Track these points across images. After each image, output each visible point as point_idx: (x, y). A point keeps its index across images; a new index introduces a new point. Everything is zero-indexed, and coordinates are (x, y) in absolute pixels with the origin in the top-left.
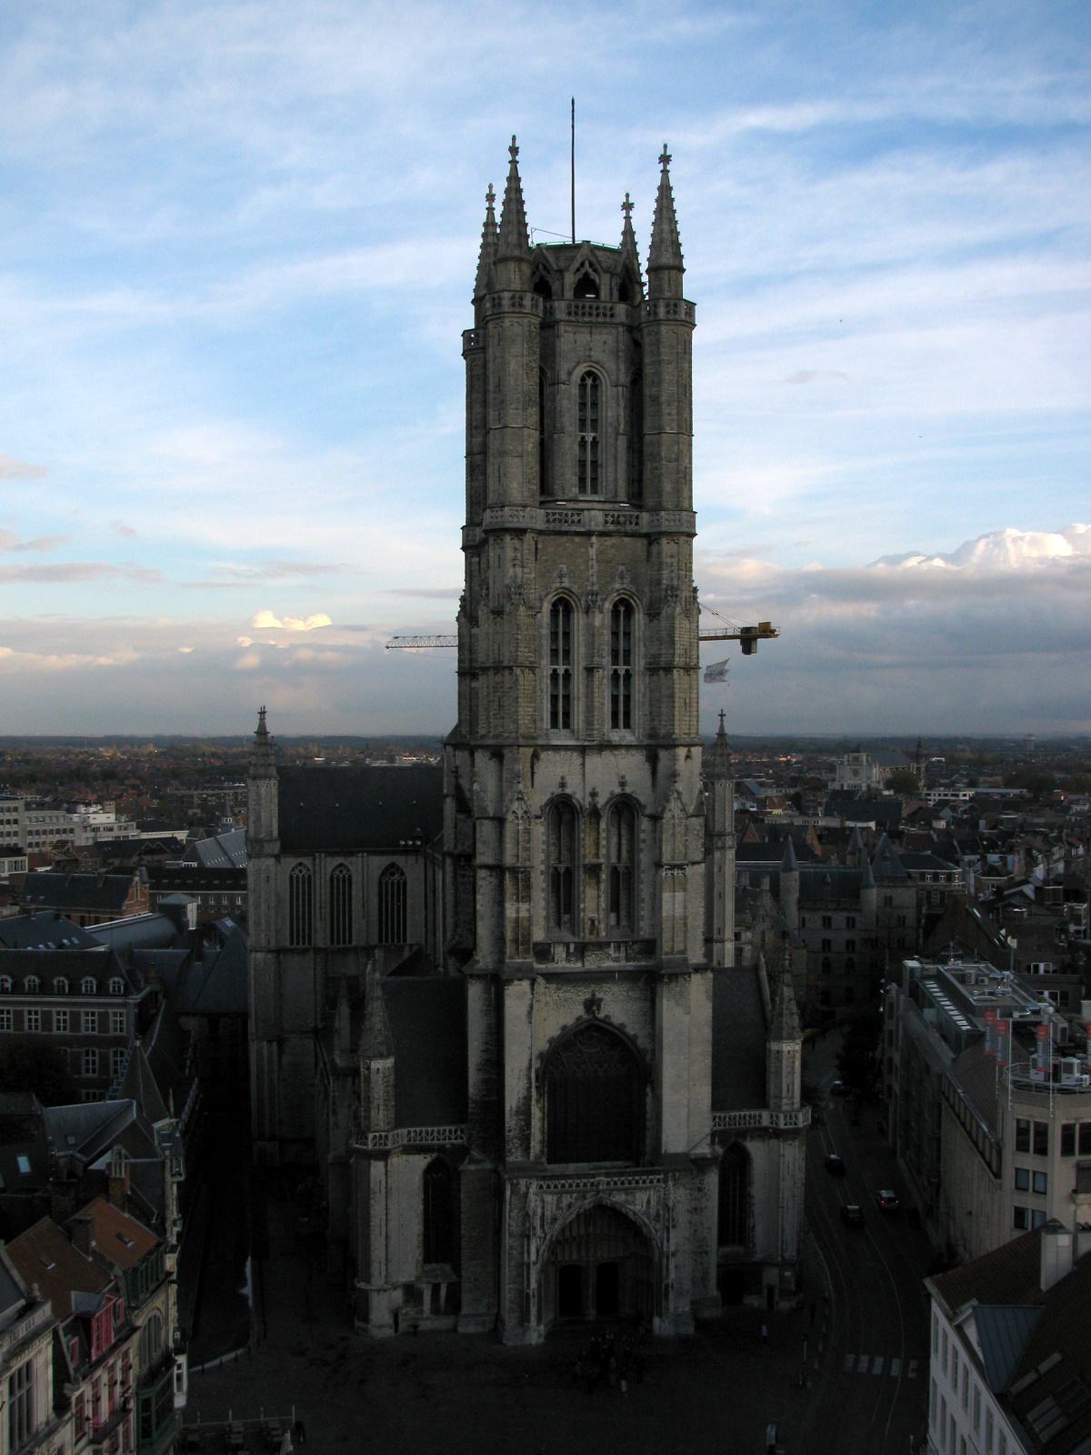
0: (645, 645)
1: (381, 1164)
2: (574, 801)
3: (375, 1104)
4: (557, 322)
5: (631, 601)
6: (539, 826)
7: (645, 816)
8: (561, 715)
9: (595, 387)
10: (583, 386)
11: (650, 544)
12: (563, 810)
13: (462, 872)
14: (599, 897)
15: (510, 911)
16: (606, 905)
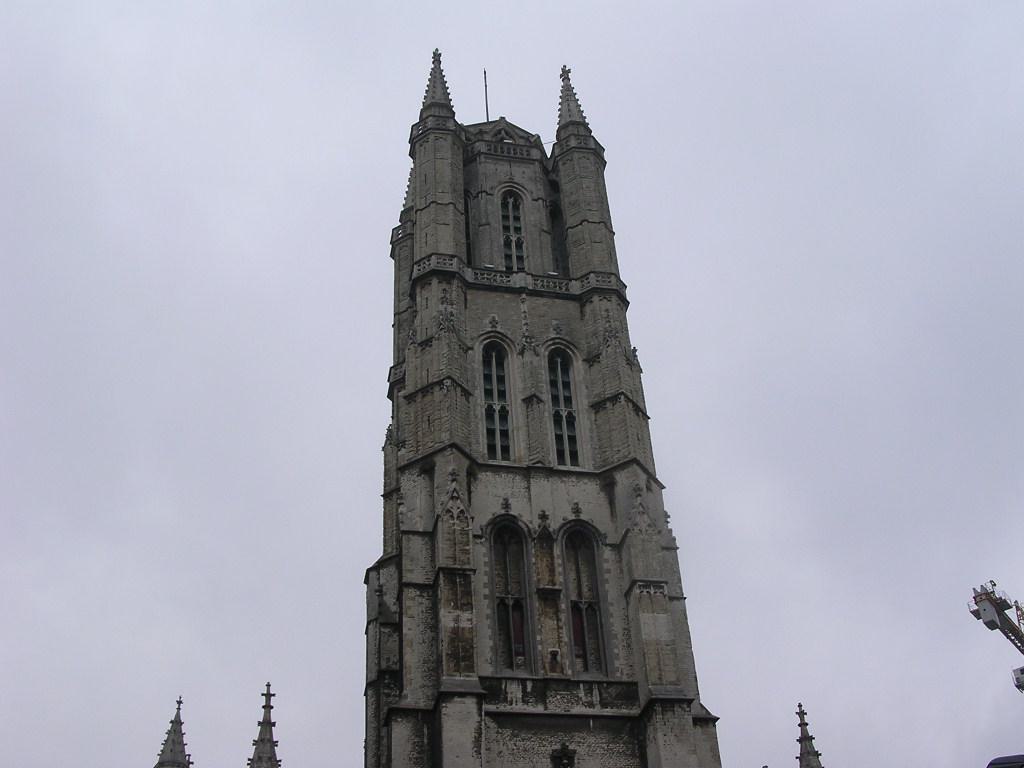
0: (587, 387)
2: (520, 523)
4: (480, 153)
6: (480, 546)
7: (606, 545)
8: (499, 439)
9: (516, 207)
10: (505, 205)
11: (582, 306)
12: (506, 532)
13: (386, 691)
14: (559, 628)
15: (447, 618)
16: (570, 639)
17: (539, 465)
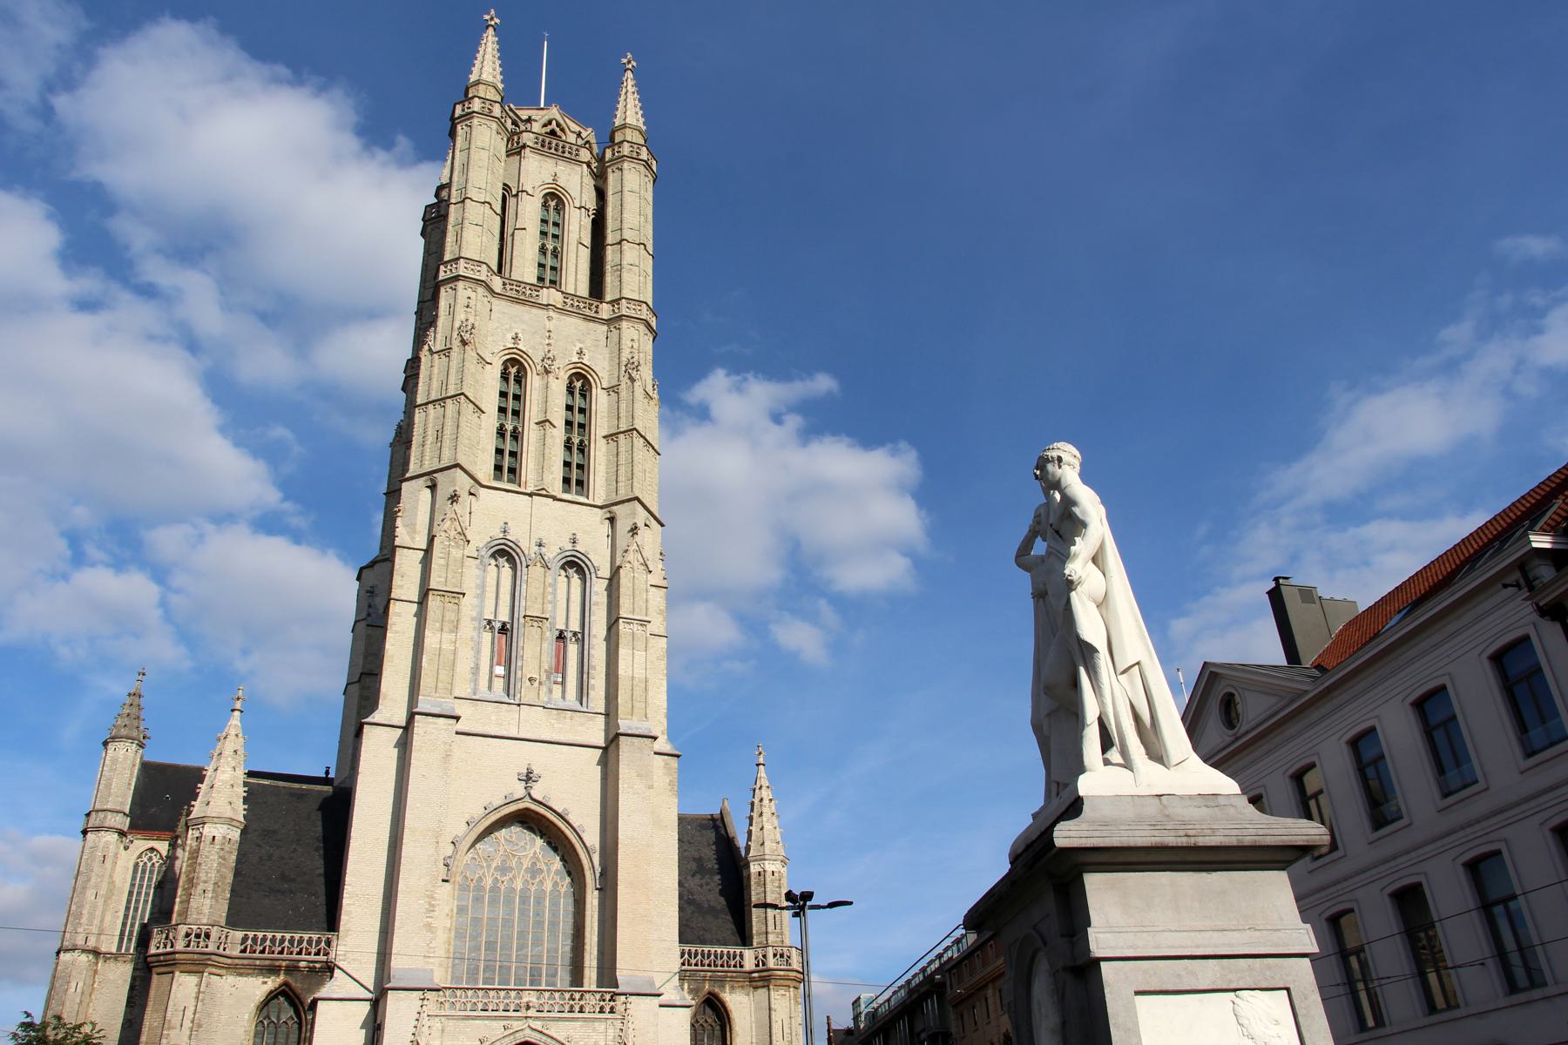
1: (193, 979)
3: (201, 887)
4: (524, 146)
5: (589, 376)
8: (508, 466)
12: (504, 553)
17: (544, 492)
